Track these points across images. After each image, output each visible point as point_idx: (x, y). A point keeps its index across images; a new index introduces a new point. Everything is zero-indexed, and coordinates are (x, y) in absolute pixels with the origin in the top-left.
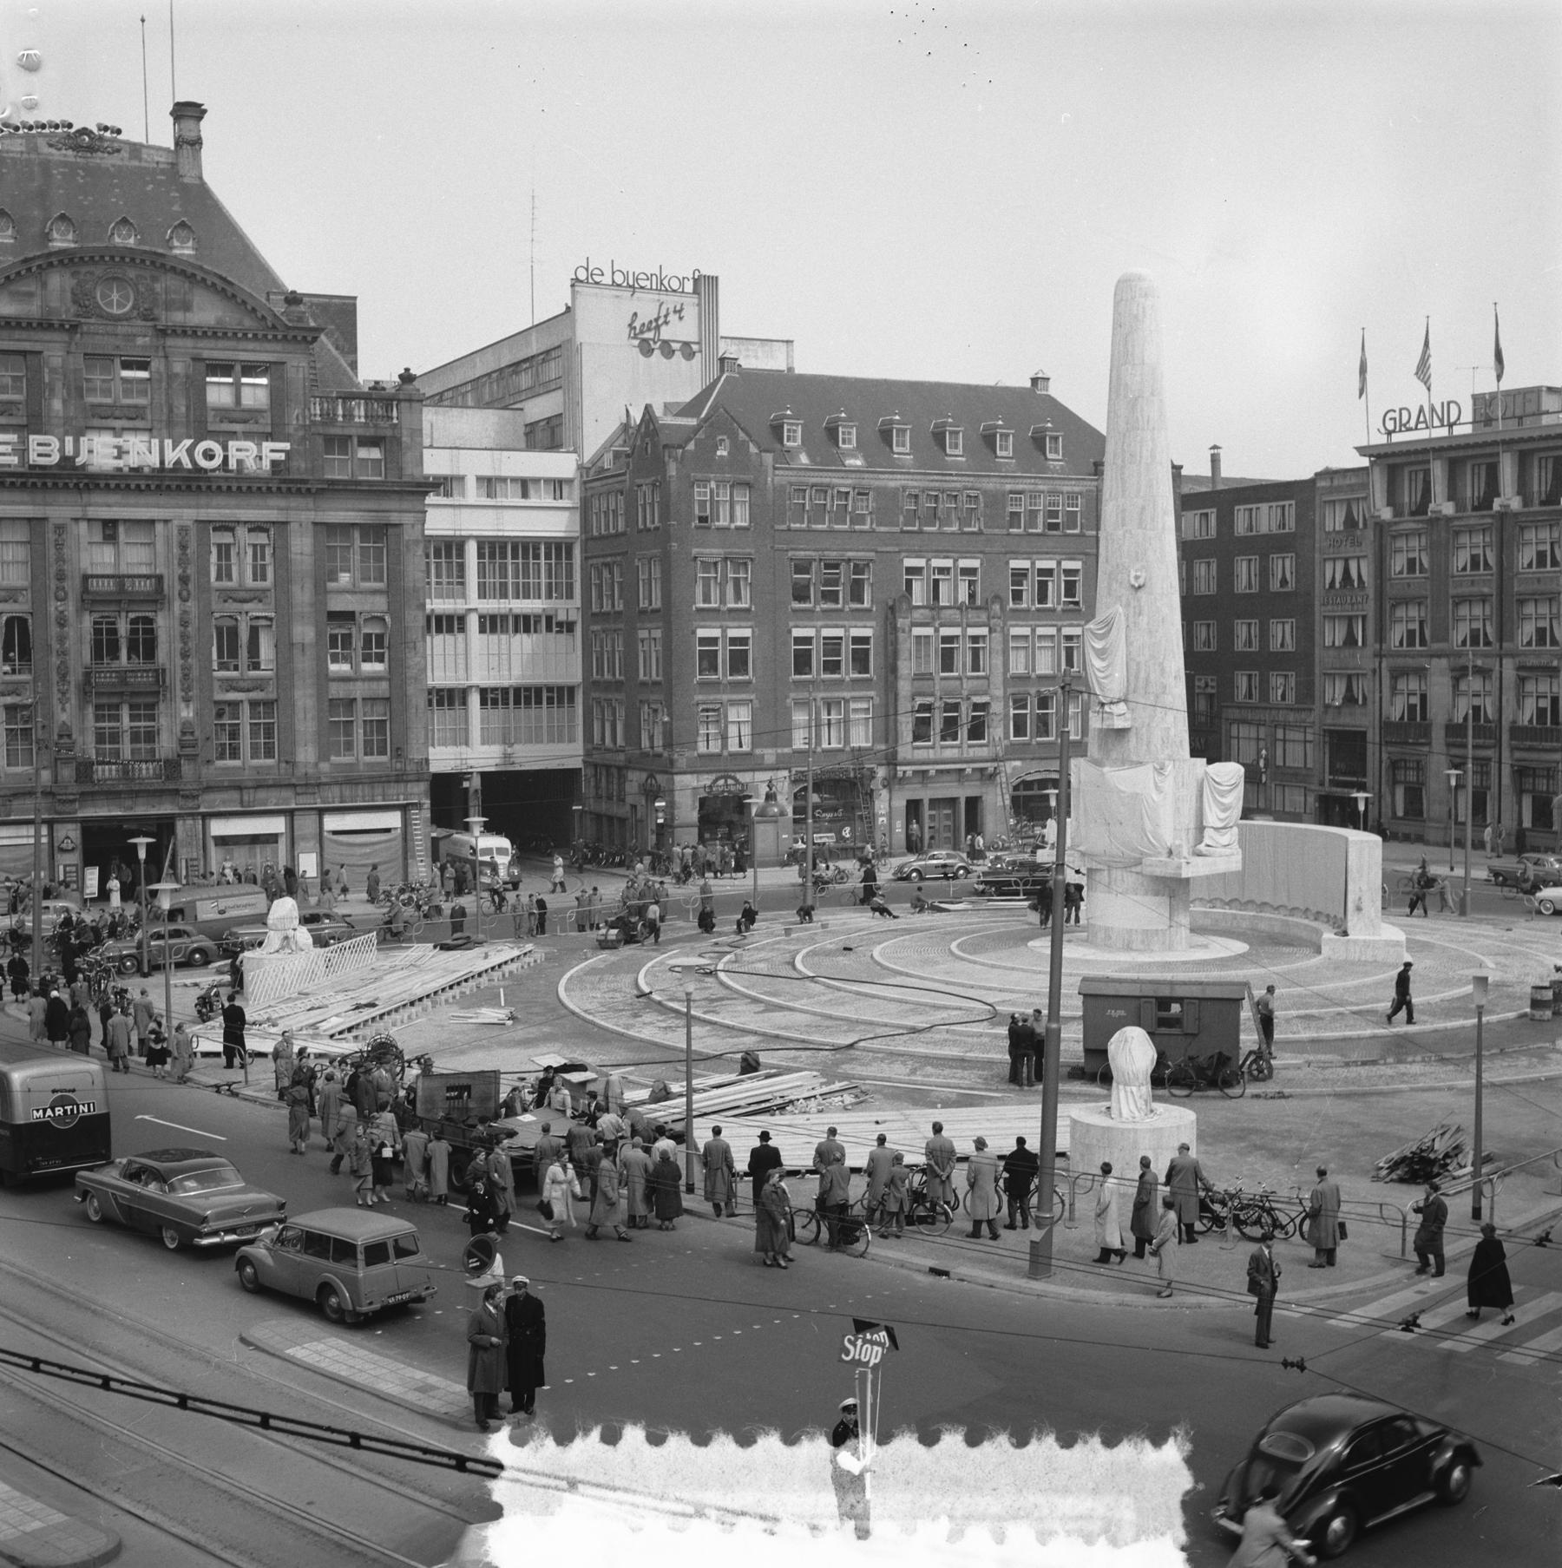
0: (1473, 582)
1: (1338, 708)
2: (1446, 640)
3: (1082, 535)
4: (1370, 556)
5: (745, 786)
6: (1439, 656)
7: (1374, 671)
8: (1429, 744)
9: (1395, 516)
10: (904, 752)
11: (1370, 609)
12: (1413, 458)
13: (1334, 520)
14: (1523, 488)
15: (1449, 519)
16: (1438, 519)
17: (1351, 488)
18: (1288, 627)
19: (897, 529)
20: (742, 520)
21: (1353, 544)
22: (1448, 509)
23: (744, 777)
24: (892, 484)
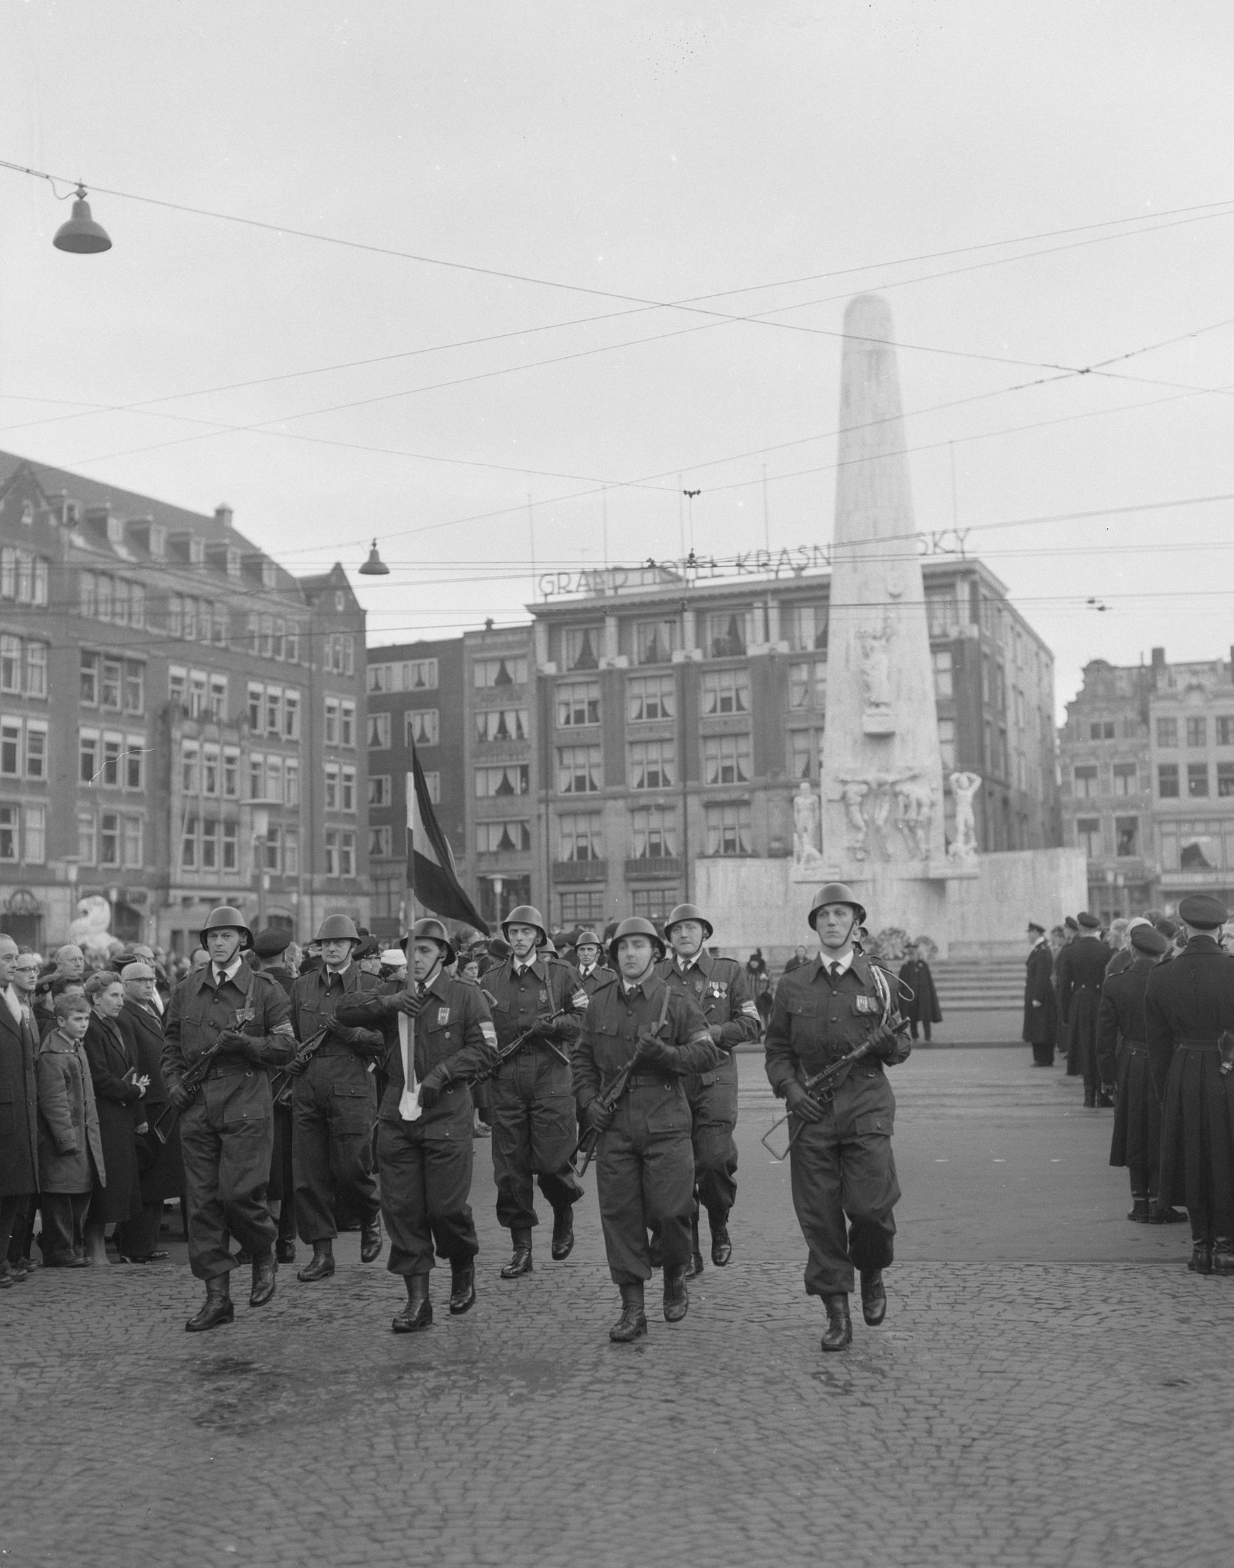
0: (651, 729)
1: (496, 854)
2: (622, 782)
3: (298, 665)
5: (39, 905)
6: (614, 797)
7: (539, 817)
8: (605, 881)
10: (178, 873)
11: (532, 758)
13: (485, 676)
14: (699, 643)
15: (622, 672)
16: (611, 672)
17: (509, 646)
19: (164, 633)
20: (41, 598)
21: (511, 698)
22: (622, 663)
23: (40, 893)
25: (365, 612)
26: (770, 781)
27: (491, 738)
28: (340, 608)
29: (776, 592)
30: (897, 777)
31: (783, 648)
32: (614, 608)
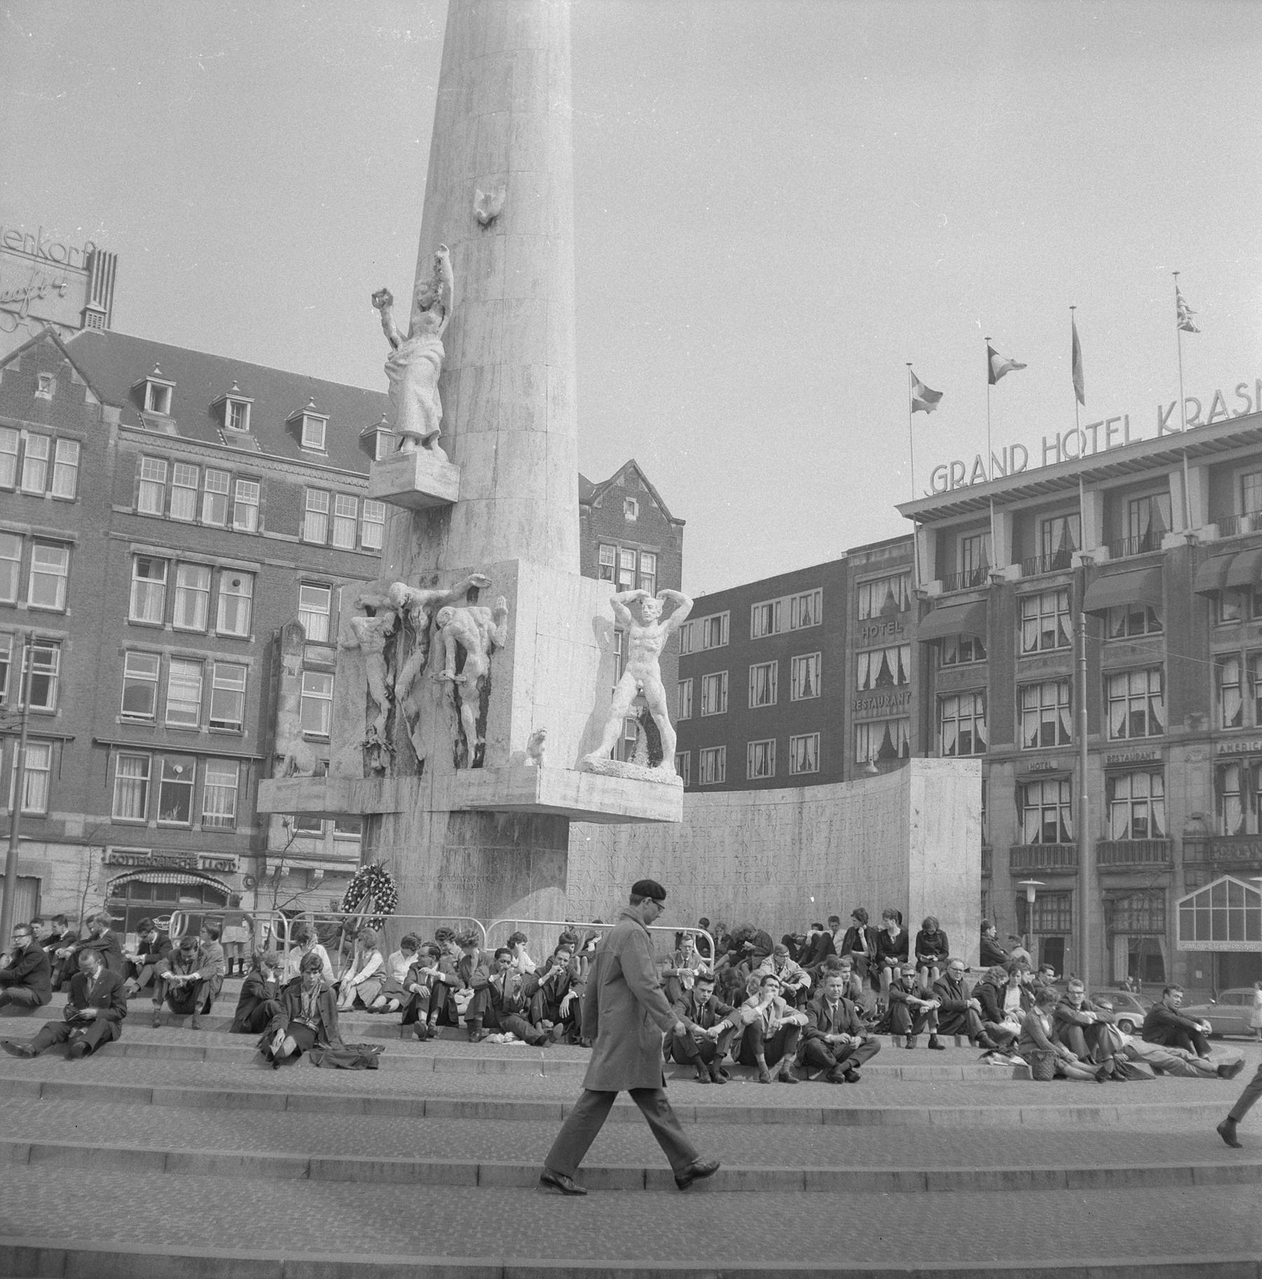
0: (1045, 664)
2: (1010, 739)
4: (916, 645)
6: (1002, 761)
9: (946, 588)
12: (968, 517)
14: (1109, 538)
17: (892, 562)
18: (811, 742)
19: (295, 539)
20: (63, 488)
22: (1013, 573)
24: (291, 479)
25: (683, 523)
26: (1188, 729)
27: (873, 685)
28: (631, 517)
29: (1194, 453)
30: (444, 592)
31: (1209, 534)
32: (1001, 500)
